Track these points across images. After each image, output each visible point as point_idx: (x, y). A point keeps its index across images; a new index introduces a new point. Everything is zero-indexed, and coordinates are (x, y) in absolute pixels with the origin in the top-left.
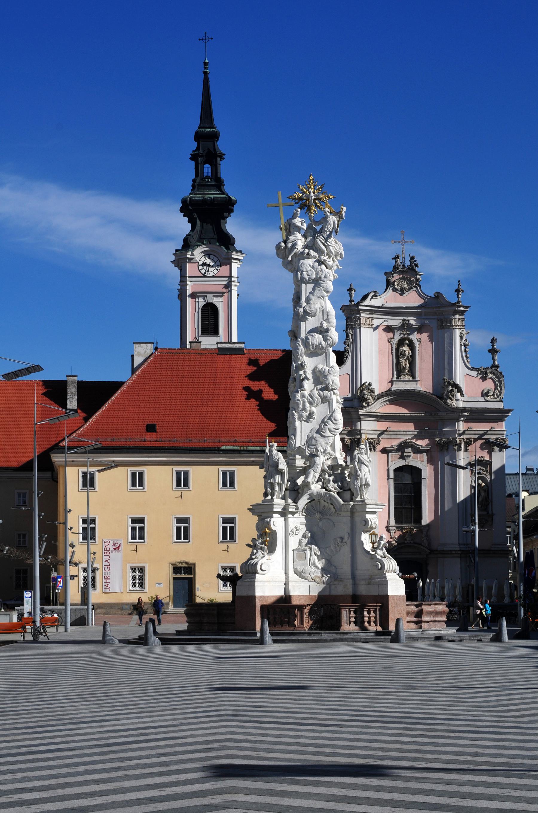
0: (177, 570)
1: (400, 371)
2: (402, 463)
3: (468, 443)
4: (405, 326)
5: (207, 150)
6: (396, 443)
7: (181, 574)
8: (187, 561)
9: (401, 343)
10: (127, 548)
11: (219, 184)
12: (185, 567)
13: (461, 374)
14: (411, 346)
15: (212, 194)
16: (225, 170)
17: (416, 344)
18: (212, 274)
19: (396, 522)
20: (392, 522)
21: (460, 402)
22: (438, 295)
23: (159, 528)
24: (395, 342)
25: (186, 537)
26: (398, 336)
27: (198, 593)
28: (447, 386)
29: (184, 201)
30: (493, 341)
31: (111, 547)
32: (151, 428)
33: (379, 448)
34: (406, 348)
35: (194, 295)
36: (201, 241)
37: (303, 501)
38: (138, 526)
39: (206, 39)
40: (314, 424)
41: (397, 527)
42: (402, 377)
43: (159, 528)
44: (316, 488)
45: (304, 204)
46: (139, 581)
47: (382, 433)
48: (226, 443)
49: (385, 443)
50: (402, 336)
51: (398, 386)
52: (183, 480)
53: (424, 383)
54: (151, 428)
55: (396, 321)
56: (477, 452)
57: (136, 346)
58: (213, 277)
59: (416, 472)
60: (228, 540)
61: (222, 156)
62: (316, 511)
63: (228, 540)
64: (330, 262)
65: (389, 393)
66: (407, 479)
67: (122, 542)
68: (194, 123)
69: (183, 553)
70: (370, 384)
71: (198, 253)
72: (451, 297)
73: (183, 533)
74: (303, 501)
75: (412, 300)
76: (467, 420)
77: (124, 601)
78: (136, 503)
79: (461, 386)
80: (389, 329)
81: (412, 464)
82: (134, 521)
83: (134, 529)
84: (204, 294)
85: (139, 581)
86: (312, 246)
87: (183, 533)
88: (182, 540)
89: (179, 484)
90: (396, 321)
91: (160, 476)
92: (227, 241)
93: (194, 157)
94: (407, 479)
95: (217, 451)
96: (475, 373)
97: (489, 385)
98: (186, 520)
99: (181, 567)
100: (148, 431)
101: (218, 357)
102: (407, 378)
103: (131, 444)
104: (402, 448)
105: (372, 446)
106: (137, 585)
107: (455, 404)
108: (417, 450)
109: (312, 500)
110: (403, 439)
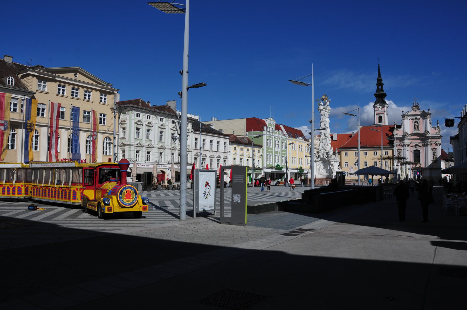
1: (415, 128)
3: (431, 144)
4: (416, 119)
6: (414, 145)
9: (415, 122)
11: (382, 90)
13: (429, 128)
14: (418, 123)
15: (380, 92)
16: (384, 87)
21: (429, 135)
22: (424, 111)
26: (414, 121)
30: (438, 121)
34: (417, 124)
35: (377, 114)
36: (378, 103)
37: (319, 159)
39: (379, 59)
40: (323, 144)
44: (322, 156)
45: (323, 100)
47: (411, 143)
49: (411, 145)
51: (414, 132)
52: (366, 154)
53: (421, 131)
56: (434, 146)
59: (419, 151)
61: (383, 84)
62: (323, 160)
64: (327, 111)
65: (412, 134)
66: (417, 152)
68: (376, 77)
71: (377, 105)
72: (427, 111)
74: (319, 159)
75: (418, 112)
76: (431, 139)
80: (412, 119)
84: (379, 114)
86: (324, 108)
90: (414, 118)
92: (385, 103)
93: (377, 85)
94: (417, 152)
95: (373, 147)
97: (437, 131)
98: (367, 162)
104: (415, 146)
105: (408, 145)
107: (428, 135)
108: (419, 146)
109: (321, 159)
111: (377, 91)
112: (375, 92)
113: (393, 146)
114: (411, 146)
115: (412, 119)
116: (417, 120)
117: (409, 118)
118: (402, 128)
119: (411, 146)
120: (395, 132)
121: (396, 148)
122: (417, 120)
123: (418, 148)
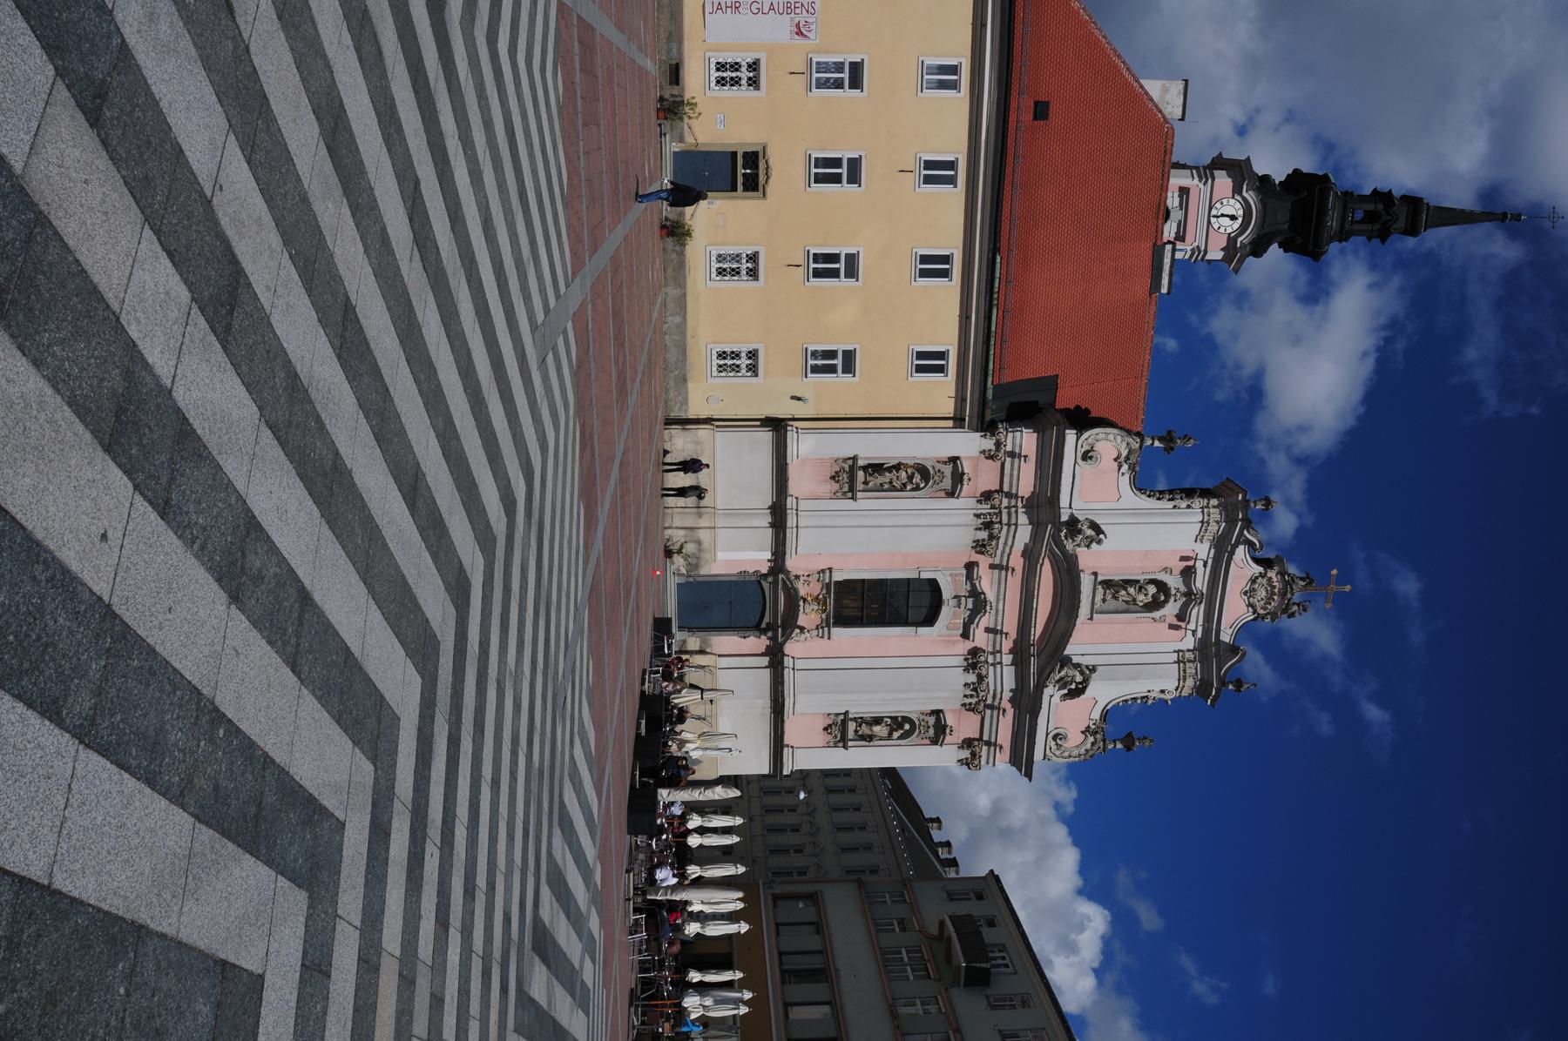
0: (752, 159)
1: (1107, 584)
2: (947, 593)
8: (771, 181)
9: (1162, 587)
10: (798, 53)
11: (1343, 236)
12: (757, 176)
14: (1155, 605)
15: (1332, 222)
17: (1157, 614)
19: (837, 583)
20: (838, 577)
23: (840, 122)
25: (820, 179)
26: (1174, 582)
28: (1082, 673)
29: (1325, 178)
31: (802, 18)
32: (1041, 110)
33: (975, 557)
38: (846, 75)
41: (828, 586)
42: (1100, 589)
43: (840, 122)
46: (728, 75)
50: (1173, 592)
51: (1086, 583)
55: (1201, 582)
57: (1181, 85)
58: (1209, 222)
59: (930, 619)
63: (813, 266)
67: (814, 38)
69: (787, 170)
70: (1099, 542)
73: (829, 171)
77: (686, 44)
81: (944, 609)
83: (839, 67)
85: (728, 75)
87: (829, 171)
89: (929, 165)
90: (1201, 582)
91: (947, 126)
95: (994, 246)
96: (1096, 715)
98: (854, 178)
99: (757, 167)
100: (1036, 103)
101: (1149, 245)
103: (1016, 65)
104: (975, 594)
110: (991, 596)
113: (986, 426)
114: (970, 567)
115: (1188, 573)
116: (1171, 609)
117: (1204, 550)
118: (1132, 500)
119: (970, 567)
120: (1109, 444)
121: (968, 444)
122: (1171, 609)
123: (950, 615)
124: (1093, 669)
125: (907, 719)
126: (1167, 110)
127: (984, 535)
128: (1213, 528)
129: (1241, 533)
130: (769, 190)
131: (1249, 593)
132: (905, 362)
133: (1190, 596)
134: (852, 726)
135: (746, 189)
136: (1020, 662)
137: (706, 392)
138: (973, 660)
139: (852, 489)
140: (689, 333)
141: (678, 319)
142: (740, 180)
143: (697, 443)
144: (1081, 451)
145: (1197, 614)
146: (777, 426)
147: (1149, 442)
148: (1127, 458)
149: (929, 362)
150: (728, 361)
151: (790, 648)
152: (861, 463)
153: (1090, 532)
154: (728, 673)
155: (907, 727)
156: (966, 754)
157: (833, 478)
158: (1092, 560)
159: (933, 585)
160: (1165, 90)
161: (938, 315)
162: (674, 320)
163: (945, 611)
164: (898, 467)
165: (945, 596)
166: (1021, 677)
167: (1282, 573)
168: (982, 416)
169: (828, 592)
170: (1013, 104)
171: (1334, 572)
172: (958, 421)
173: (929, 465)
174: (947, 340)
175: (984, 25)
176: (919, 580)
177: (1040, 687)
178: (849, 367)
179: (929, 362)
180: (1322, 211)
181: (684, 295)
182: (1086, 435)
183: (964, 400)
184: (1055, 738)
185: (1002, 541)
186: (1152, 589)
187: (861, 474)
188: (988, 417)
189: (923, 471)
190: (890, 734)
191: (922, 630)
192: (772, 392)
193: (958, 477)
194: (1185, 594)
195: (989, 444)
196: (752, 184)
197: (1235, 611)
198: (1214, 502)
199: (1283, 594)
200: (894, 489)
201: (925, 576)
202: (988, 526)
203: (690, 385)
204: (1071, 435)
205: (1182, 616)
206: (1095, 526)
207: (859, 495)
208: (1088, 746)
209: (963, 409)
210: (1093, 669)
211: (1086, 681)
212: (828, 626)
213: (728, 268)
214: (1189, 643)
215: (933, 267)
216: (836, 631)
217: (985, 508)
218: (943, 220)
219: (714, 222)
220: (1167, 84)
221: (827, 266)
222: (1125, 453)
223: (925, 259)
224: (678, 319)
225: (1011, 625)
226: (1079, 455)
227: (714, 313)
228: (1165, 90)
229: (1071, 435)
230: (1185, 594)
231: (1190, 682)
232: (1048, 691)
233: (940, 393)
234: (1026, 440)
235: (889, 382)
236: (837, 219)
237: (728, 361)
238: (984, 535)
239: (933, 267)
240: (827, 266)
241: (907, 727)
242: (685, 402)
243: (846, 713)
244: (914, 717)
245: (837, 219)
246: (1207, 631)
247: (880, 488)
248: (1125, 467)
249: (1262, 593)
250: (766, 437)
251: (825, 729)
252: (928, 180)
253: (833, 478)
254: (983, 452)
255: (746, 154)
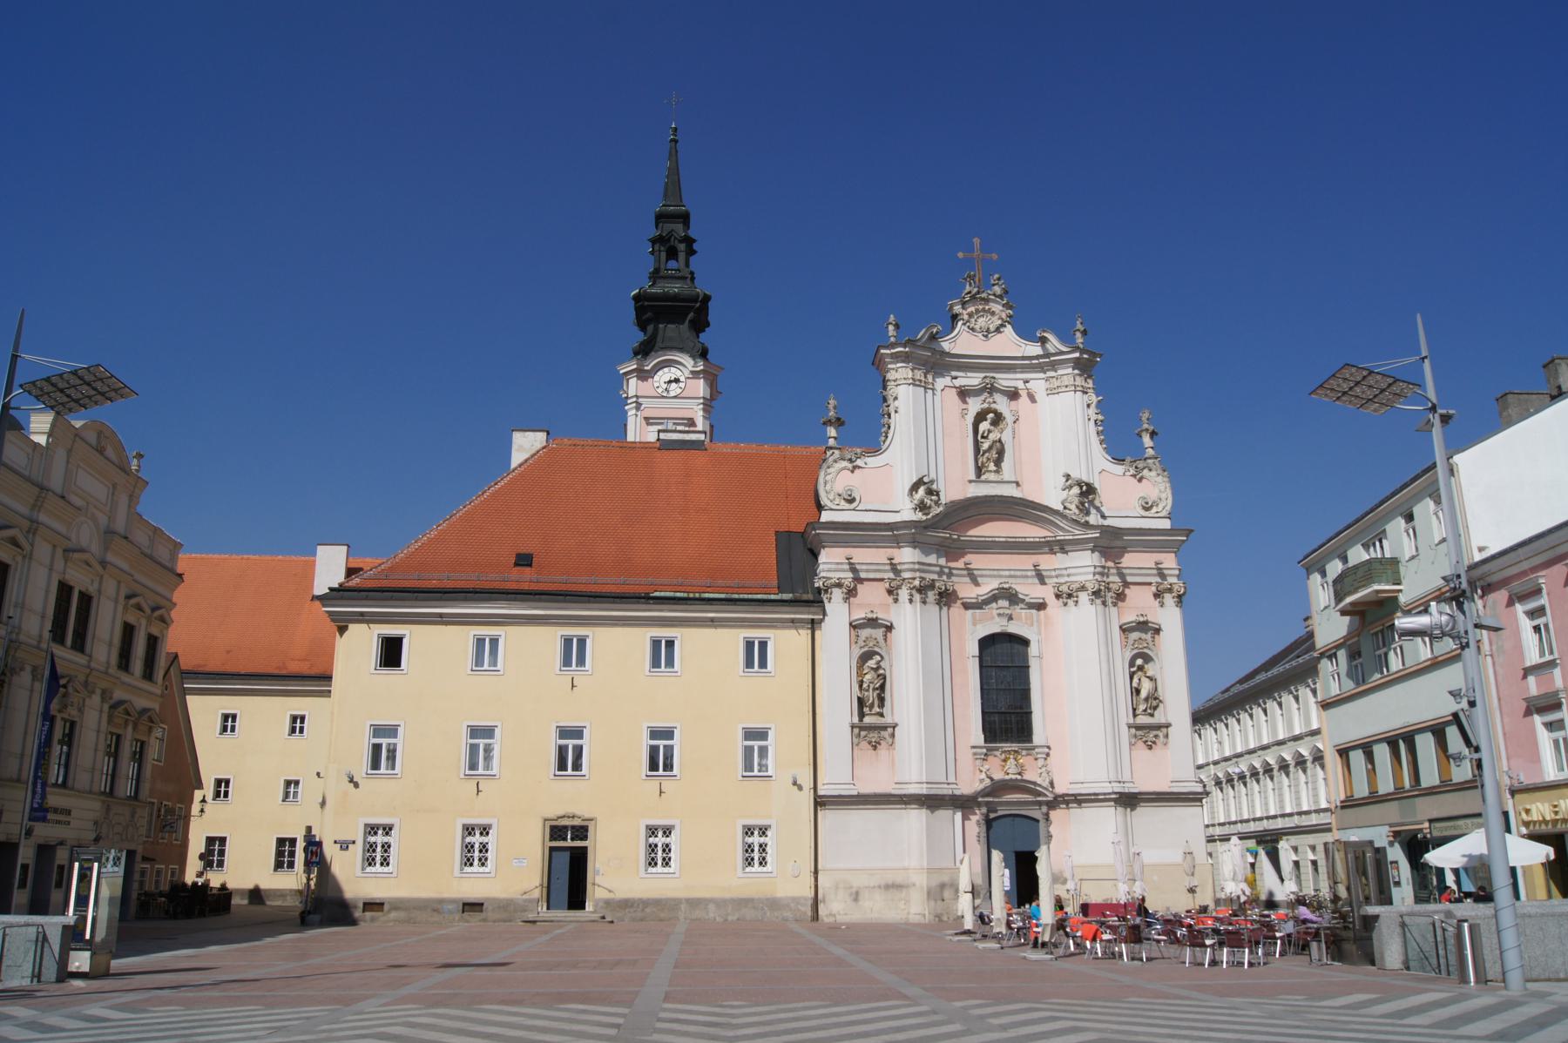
0: (557, 832)
1: (979, 470)
2: (995, 626)
5: (673, 238)
7: (565, 839)
8: (578, 813)
12: (573, 827)
15: (675, 288)
17: (1009, 418)
18: (672, 394)
20: (979, 738)
23: (524, 752)
24: (970, 418)
26: (975, 405)
27: (598, 880)
28: (1071, 487)
32: (524, 560)
46: (474, 854)
48: (663, 587)
52: (574, 653)
54: (524, 560)
55: (973, 380)
60: (661, 772)
63: (661, 772)
73: (568, 760)
77: (446, 895)
78: (479, 697)
79: (1096, 485)
82: (475, 732)
85: (474, 854)
87: (568, 760)
88: (570, 771)
89: (567, 662)
90: (973, 380)
91: (530, 645)
95: (646, 599)
96: (1119, 469)
98: (577, 733)
99: (566, 827)
100: (516, 564)
101: (658, 454)
102: (992, 477)
104: (993, 598)
106: (476, 862)
111: (656, 276)
112: (640, 283)
115: (964, 394)
116: (1002, 404)
120: (835, 480)
121: (837, 612)
122: (1002, 404)
124: (1068, 477)
125: (1132, 664)
126: (538, 445)
127: (932, 596)
128: (919, 375)
129: (923, 347)
130: (587, 816)
131: (987, 333)
132: (755, 678)
133: (990, 389)
134: (1143, 720)
135: (585, 838)
136: (1062, 547)
137: (784, 877)
138: (1066, 596)
139: (885, 728)
140: (727, 895)
141: (712, 907)
142: (578, 843)
143: (837, 888)
144: (844, 505)
145: (1005, 380)
146: (820, 802)
147: (831, 442)
148: (850, 460)
149: (755, 655)
150: (753, 855)
151: (1060, 789)
152: (856, 720)
153: (922, 491)
154: (1085, 857)
155: (1139, 662)
156: (1169, 599)
157: (875, 748)
158: (957, 485)
159: (987, 643)
160: (521, 448)
161: (709, 648)
162: (712, 913)
163: (1013, 628)
164: (861, 683)
165: (997, 630)
166: (1077, 544)
167: (964, 304)
168: (808, 603)
169: (997, 749)
170: (514, 586)
171: (960, 255)
172: (814, 625)
173: (857, 652)
174: (733, 640)
175: (441, 615)
176: (981, 657)
177: (1087, 525)
178: (761, 734)
179: (755, 655)
180: (666, 297)
181: (688, 901)
182: (824, 501)
183: (792, 621)
184: (1147, 509)
185: (935, 577)
186: (984, 426)
187: (867, 720)
188: (810, 597)
189: (865, 657)
190: (1150, 678)
191: (1033, 650)
192: (785, 809)
193: (872, 622)
194: (991, 394)
195: (837, 594)
196: (581, 832)
197: (1008, 344)
198: (891, 376)
199: (987, 301)
200: (882, 687)
201: (974, 649)
202: (921, 590)
203: (780, 893)
204: (826, 517)
205: (1013, 395)
206: (915, 488)
207: (888, 720)
208: (1153, 474)
209: (801, 621)
210: (1068, 477)
211: (1079, 484)
212: (1033, 748)
213: (657, 856)
214: (1038, 383)
215: (662, 654)
216: (1038, 738)
217: (904, 594)
218: (618, 645)
219: (615, 874)
220: (514, 447)
221: (659, 761)
222: (845, 464)
223: (749, 663)
224: (712, 907)
225: (1025, 562)
226: (847, 506)
227: (705, 871)
228: (521, 448)
229: (826, 517)
230: (991, 394)
231: (1080, 381)
232: (1093, 519)
233: (787, 643)
234: (831, 562)
235: (775, 696)
236: (615, 750)
237: (753, 855)
238: (932, 596)
239: (662, 654)
240: (659, 761)
241: (1139, 662)
242: (796, 900)
243: (1130, 727)
244: (1129, 655)
245: (615, 750)
246: (1024, 369)
247: (882, 700)
248: (859, 462)
249: (982, 322)
250: (827, 817)
251: (1150, 748)
252: (581, 661)
253: (875, 748)
254: (846, 600)
255: (552, 838)
